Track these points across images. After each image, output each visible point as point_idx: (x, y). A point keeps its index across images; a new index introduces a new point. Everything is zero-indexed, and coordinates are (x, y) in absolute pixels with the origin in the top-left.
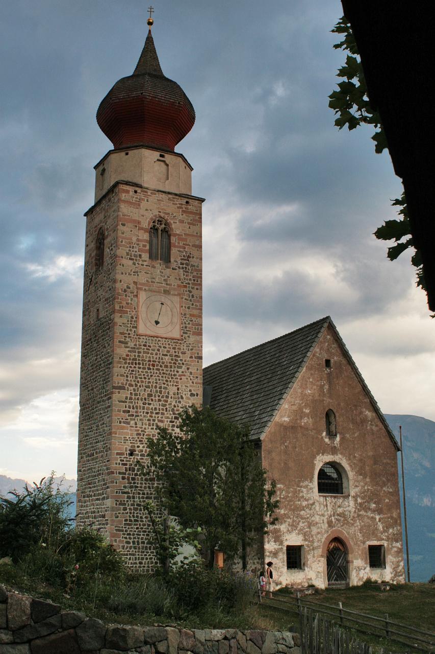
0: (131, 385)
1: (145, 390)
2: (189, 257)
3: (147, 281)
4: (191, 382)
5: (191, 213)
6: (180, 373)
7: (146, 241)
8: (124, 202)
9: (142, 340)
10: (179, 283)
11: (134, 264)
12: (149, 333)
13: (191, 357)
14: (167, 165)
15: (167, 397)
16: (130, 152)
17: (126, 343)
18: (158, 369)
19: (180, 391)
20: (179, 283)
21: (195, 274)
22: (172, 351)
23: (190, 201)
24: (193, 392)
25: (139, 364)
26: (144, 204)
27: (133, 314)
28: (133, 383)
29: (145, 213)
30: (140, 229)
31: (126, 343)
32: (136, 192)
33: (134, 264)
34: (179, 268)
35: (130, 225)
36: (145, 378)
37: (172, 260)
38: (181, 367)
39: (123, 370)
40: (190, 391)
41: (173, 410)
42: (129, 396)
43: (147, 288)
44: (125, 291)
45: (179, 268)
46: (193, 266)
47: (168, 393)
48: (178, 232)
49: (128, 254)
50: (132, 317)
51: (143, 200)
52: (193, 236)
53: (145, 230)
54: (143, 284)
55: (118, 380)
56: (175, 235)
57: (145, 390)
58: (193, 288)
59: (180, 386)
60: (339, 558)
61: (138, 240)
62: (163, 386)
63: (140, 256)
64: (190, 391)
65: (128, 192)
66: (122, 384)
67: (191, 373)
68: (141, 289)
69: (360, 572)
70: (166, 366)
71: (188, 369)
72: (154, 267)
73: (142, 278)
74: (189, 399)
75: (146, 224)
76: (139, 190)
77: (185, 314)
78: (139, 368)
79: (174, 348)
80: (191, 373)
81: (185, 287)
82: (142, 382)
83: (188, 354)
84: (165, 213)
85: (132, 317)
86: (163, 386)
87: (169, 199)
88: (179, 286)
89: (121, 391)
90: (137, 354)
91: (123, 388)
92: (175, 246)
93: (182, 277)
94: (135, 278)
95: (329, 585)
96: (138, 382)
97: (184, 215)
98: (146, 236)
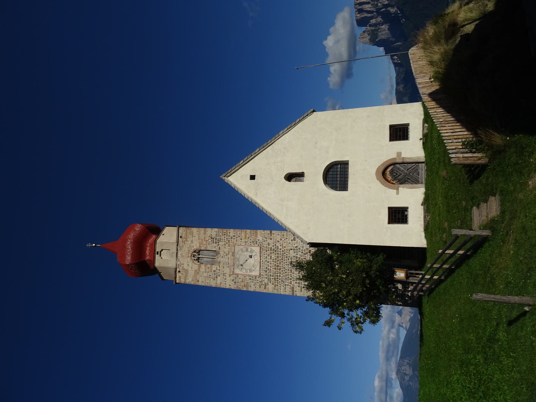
0: (291, 283)
1: (293, 273)
2: (211, 238)
3: (228, 267)
4: (286, 240)
5: (186, 235)
6: (281, 247)
7: (205, 266)
9: (263, 273)
10: (227, 245)
11: (219, 275)
12: (258, 268)
13: (271, 239)
14: (162, 250)
16: (160, 271)
18: (280, 263)
19: (292, 248)
21: (221, 234)
22: (268, 252)
23: (180, 235)
24: (292, 239)
25: (277, 276)
26: (185, 267)
27: (248, 278)
28: (289, 281)
29: (190, 265)
30: (199, 269)
32: (179, 272)
33: (219, 275)
34: (218, 245)
35: (198, 277)
36: (286, 273)
37: (214, 250)
39: (282, 288)
40: (292, 240)
41: (305, 254)
42: (297, 285)
44: (235, 283)
45: (218, 245)
46: (216, 235)
47: (294, 256)
48: (198, 245)
49: (214, 280)
50: (250, 279)
51: (183, 267)
52: (199, 234)
53: (200, 267)
54: (230, 270)
55: (288, 292)
57: (293, 273)
58: (229, 236)
59: (290, 248)
61: (205, 272)
63: (214, 271)
64: (292, 240)
65: (180, 277)
66: (290, 288)
68: (233, 272)
70: (278, 257)
71: (278, 242)
72: (220, 262)
73: (227, 271)
74: (297, 241)
75: (195, 266)
76: (178, 270)
77: (245, 242)
78: (280, 276)
79: (266, 251)
80: (281, 239)
81: (229, 241)
82: (288, 275)
83: (269, 241)
84: (189, 253)
85: (250, 279)
87: (181, 250)
88: (229, 246)
90: (272, 277)
91: (293, 288)
92: (206, 247)
94: (227, 275)
98: (203, 266)
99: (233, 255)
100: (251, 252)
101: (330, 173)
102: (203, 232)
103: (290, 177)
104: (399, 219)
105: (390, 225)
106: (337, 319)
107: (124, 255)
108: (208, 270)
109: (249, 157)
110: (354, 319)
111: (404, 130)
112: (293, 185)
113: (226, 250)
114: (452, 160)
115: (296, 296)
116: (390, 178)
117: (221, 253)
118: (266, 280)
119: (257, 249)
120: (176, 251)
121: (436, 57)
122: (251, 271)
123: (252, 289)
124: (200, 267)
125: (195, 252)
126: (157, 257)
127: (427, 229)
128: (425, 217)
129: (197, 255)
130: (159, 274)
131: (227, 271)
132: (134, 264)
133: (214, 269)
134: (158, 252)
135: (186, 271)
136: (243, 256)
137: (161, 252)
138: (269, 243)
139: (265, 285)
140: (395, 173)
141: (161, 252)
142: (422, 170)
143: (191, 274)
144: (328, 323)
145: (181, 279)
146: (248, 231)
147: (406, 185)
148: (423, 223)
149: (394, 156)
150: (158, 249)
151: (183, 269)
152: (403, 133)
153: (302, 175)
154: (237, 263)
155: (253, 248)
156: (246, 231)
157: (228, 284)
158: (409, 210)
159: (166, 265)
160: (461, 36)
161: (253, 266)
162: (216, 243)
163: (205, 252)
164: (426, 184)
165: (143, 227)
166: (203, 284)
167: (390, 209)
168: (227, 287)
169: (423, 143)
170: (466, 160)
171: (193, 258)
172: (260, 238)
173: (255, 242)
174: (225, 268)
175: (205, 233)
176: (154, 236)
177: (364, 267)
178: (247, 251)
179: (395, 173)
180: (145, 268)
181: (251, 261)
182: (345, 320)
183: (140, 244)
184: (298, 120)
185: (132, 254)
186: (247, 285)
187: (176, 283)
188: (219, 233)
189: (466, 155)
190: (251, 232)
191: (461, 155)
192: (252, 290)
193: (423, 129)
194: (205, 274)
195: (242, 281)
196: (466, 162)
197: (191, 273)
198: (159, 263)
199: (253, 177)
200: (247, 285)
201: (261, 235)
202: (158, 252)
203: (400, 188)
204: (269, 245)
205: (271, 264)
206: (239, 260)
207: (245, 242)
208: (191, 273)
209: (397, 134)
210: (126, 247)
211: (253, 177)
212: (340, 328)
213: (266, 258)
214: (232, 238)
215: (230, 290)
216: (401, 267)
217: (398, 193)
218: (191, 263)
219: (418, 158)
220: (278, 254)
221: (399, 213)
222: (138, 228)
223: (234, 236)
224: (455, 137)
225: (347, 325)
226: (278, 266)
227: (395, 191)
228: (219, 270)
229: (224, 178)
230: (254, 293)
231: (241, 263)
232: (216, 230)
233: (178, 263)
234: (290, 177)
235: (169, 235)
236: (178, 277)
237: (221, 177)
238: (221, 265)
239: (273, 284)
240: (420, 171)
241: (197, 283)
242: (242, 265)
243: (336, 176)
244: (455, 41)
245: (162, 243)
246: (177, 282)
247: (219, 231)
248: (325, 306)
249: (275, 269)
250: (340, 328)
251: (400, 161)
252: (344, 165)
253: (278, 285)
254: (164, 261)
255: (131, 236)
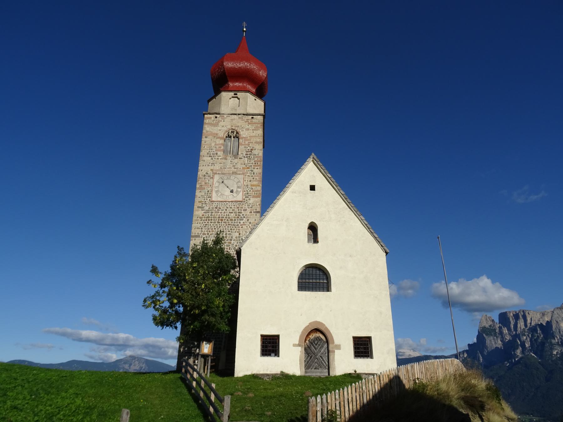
0: (204, 234)
2: (252, 150)
3: (221, 168)
5: (255, 123)
6: (242, 223)
7: (222, 144)
8: (209, 124)
9: (214, 205)
10: (244, 166)
11: (212, 159)
12: (219, 199)
13: (251, 212)
14: (239, 99)
15: (231, 240)
17: (203, 208)
19: (241, 235)
20: (244, 166)
21: (256, 159)
22: (236, 210)
23: (254, 117)
25: (211, 220)
26: (222, 123)
28: (206, 233)
29: (223, 128)
30: (219, 138)
31: (203, 208)
32: (216, 117)
33: (212, 159)
34: (244, 157)
35: (210, 137)
36: (215, 229)
38: (243, 220)
39: (199, 225)
43: (220, 172)
44: (205, 176)
45: (244, 157)
46: (254, 155)
47: (232, 237)
49: (208, 154)
50: (208, 191)
51: (221, 121)
52: (255, 136)
53: (221, 138)
55: (194, 231)
56: (242, 138)
58: (254, 168)
59: (241, 232)
60: (322, 347)
61: (216, 144)
62: (228, 233)
63: (217, 154)
65: (211, 118)
66: (198, 234)
67: (250, 223)
68: (216, 174)
69: (344, 362)
70: (231, 220)
71: (248, 220)
72: (226, 159)
73: (217, 167)
75: (222, 134)
76: (218, 116)
77: (247, 185)
78: (211, 222)
80: (250, 223)
81: (248, 168)
82: (213, 231)
83: (249, 210)
84: (236, 126)
85: (208, 191)
86: (228, 233)
87: (239, 118)
89: (197, 238)
91: (198, 236)
92: (242, 145)
93: (246, 162)
94: (212, 168)
95: (306, 372)
96: (210, 232)
97: (250, 126)
98: (222, 141)
99: (233, 173)
100: (237, 191)
101: (318, 271)
102: (258, 140)
103: (313, 228)
104: (266, 347)
105: (259, 338)
106: (158, 280)
107: (232, 59)
108: (217, 147)
109: (335, 183)
110: (158, 298)
111: (365, 353)
112: (305, 231)
113: (239, 166)
114: (313, 398)
115: (190, 240)
116: (312, 336)
117: (236, 161)
118: (207, 208)
119: (240, 197)
120: (238, 112)
121: (443, 387)
122: (217, 192)
123: (198, 193)
124: (221, 138)
125: (237, 133)
126: (232, 94)
127: (255, 377)
128: (268, 375)
129: (233, 135)
130: (214, 97)
131: (217, 167)
132: (224, 70)
133: (219, 153)
134: (236, 94)
135: (216, 125)
136: (232, 183)
137: (237, 97)
138: (246, 210)
139: (202, 207)
140: (317, 342)
141: (237, 97)
142: (321, 372)
143: (214, 130)
144: (154, 270)
145: (209, 119)
146: (259, 188)
147: (303, 355)
148: (262, 372)
149: (337, 341)
150: (239, 94)
151: (219, 121)
152: (362, 352)
153: (316, 240)
154: (225, 177)
155: (241, 193)
156: (259, 186)
157: (203, 168)
158: (276, 358)
159: (223, 103)
160: (468, 415)
161: (222, 194)
162: (246, 154)
163: (237, 144)
164: (305, 377)
165: (264, 78)
166: (203, 142)
167: (278, 337)
168: (199, 168)
169: (350, 374)
170: (312, 413)
171: (230, 131)
172: (252, 200)
173: (247, 195)
174: (220, 165)
175: (256, 142)
176: (254, 90)
177: (212, 308)
178: (238, 187)
179: (317, 342)
180: (221, 82)
181: (227, 192)
182: (158, 288)
183: (244, 76)
184: (376, 236)
185: (234, 68)
186: (202, 188)
187: (204, 114)
188: (257, 157)
189: (319, 414)
190: (258, 191)
191: (319, 408)
192: (196, 194)
193: (366, 374)
194: (213, 144)
195: (206, 183)
196: (310, 414)
197: (215, 130)
198: (225, 96)
199: (312, 188)
200: (202, 188)
201: (256, 202)
202: (236, 94)
203: (300, 348)
204: (244, 210)
205: (224, 213)
206: (228, 179)
207: (247, 185)
208: (215, 130)
209: (361, 344)
210: (241, 61)
211: (312, 188)
212: (149, 282)
213: (231, 208)
214: (252, 171)
215: (196, 170)
216: (215, 349)
217: (294, 345)
218: (225, 129)
219: (334, 368)
220: (235, 220)
221: (273, 347)
222: (262, 74)
223: (254, 173)
224: (342, 403)
225: (152, 290)
226: (222, 220)
227: (297, 343)
228: (218, 159)
229: (312, 157)
230: (193, 196)
231: (225, 181)
232: (261, 154)
233: (225, 116)
234: (313, 228)
235: (255, 105)
236: (211, 116)
237: (313, 154)
238: (223, 161)
239: (203, 215)
240: (320, 370)
241: (204, 137)
242: (223, 182)
243: (314, 278)
244: (462, 408)
245: (246, 99)
246: (206, 116)
247: (260, 157)
248: (172, 267)
249: (219, 217)
250: (149, 282)
251: (330, 349)
252: (327, 287)
253: (201, 220)
254: (227, 101)
255: (253, 66)
